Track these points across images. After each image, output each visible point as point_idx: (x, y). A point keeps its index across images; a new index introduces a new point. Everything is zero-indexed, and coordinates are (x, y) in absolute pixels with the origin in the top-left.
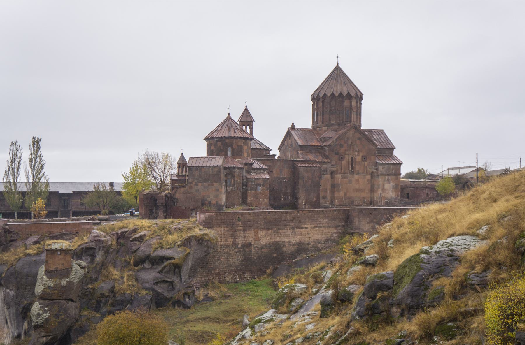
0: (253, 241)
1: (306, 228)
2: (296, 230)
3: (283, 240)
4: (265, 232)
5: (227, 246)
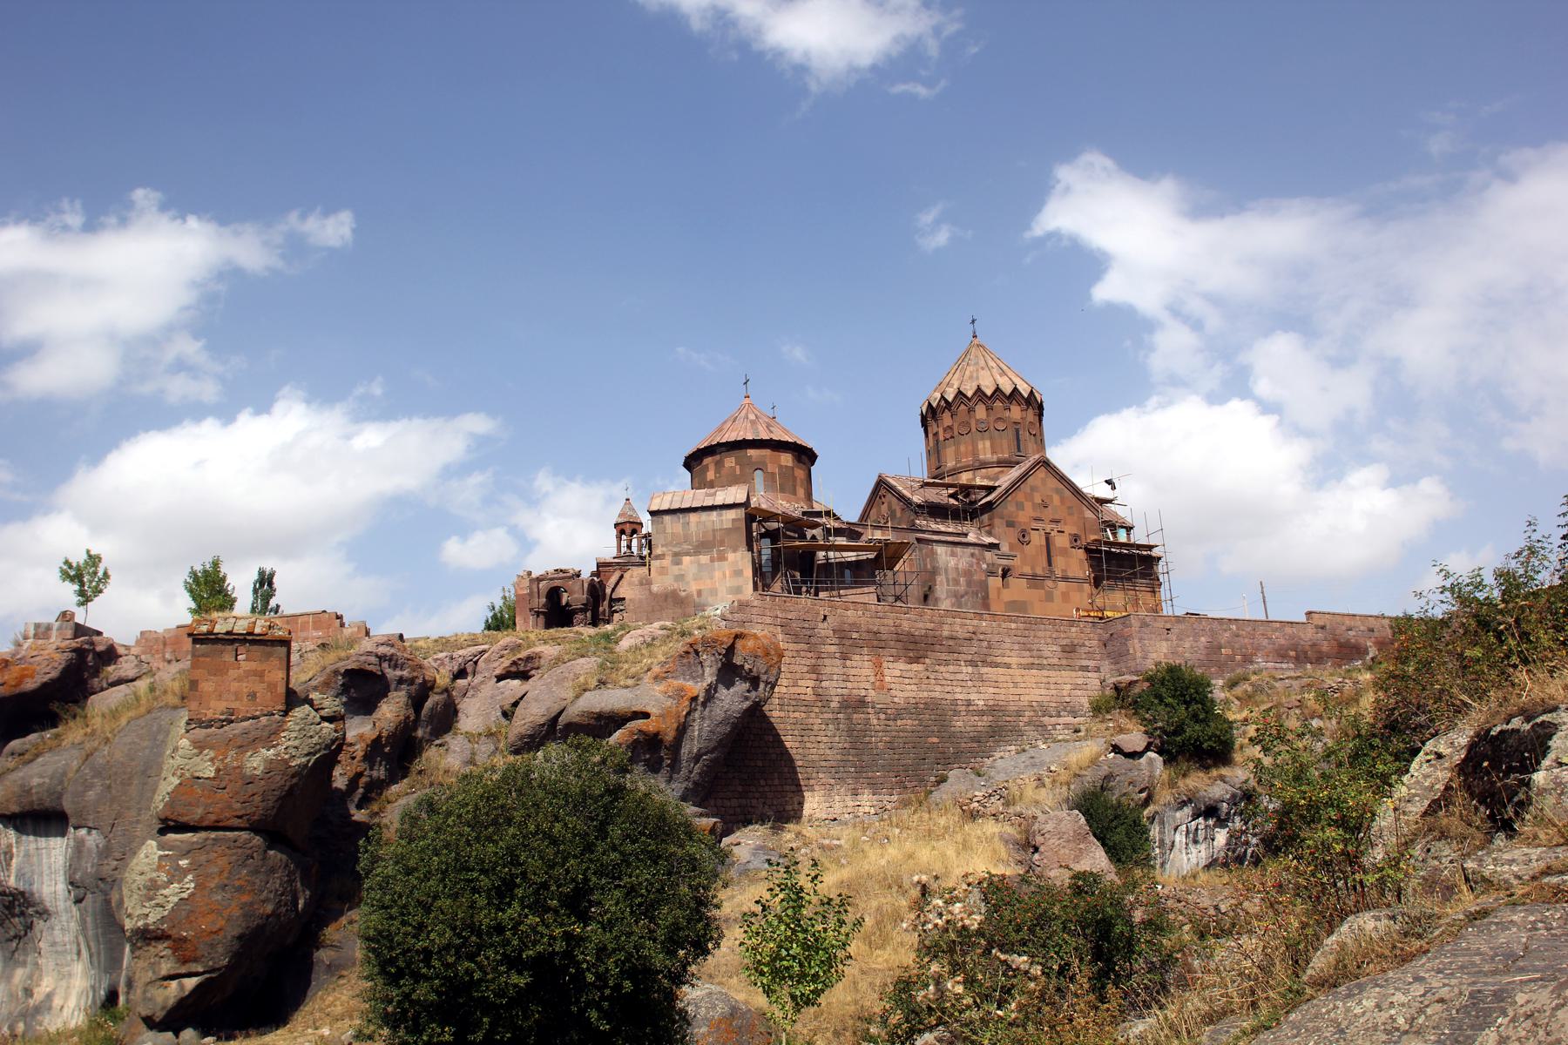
0: (872, 693)
1: (1008, 666)
2: (984, 670)
3: (948, 696)
4: (901, 665)
5: (798, 702)
